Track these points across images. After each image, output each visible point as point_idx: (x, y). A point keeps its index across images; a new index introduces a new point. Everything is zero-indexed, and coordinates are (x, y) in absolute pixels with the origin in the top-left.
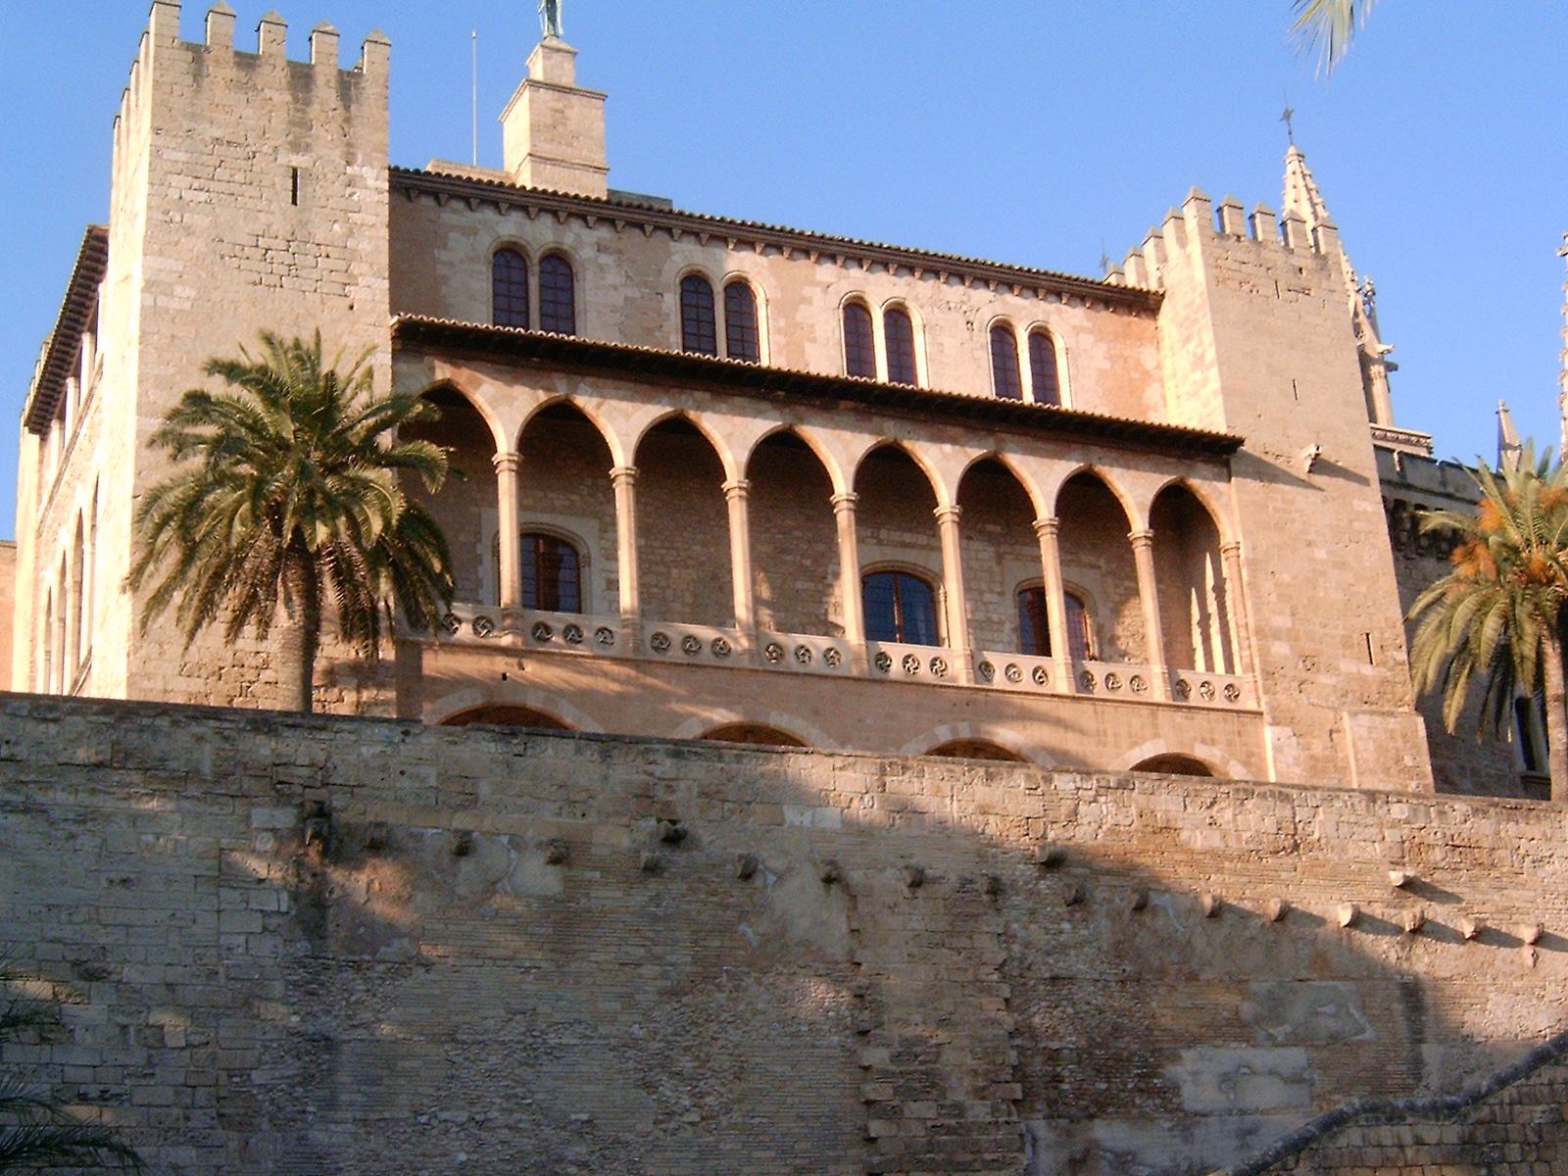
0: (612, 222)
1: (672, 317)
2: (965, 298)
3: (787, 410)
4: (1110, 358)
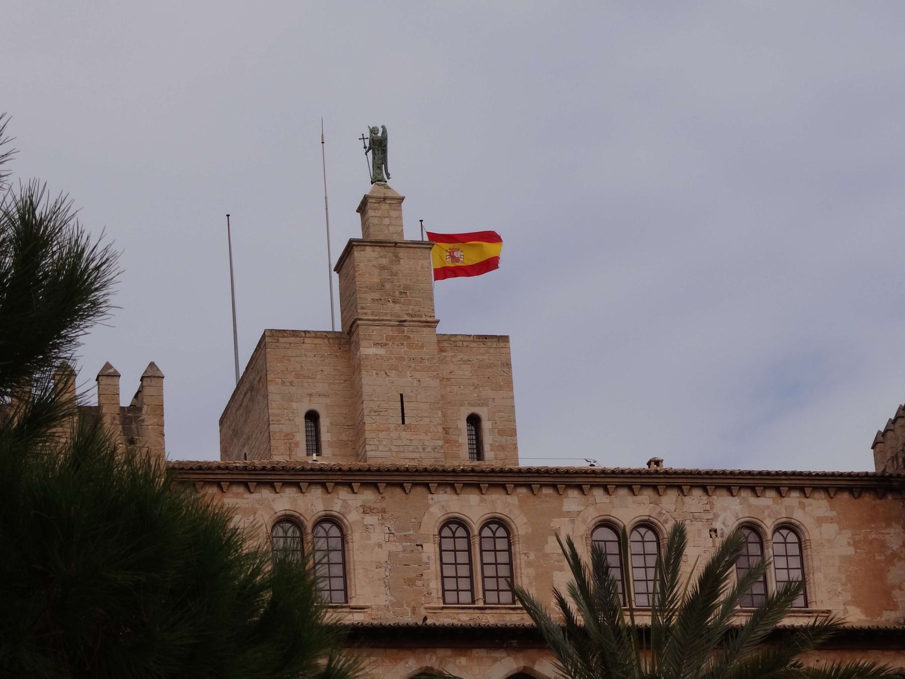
0: (374, 486)
1: (432, 563)
2: (708, 507)
3: (520, 655)
4: (855, 544)
